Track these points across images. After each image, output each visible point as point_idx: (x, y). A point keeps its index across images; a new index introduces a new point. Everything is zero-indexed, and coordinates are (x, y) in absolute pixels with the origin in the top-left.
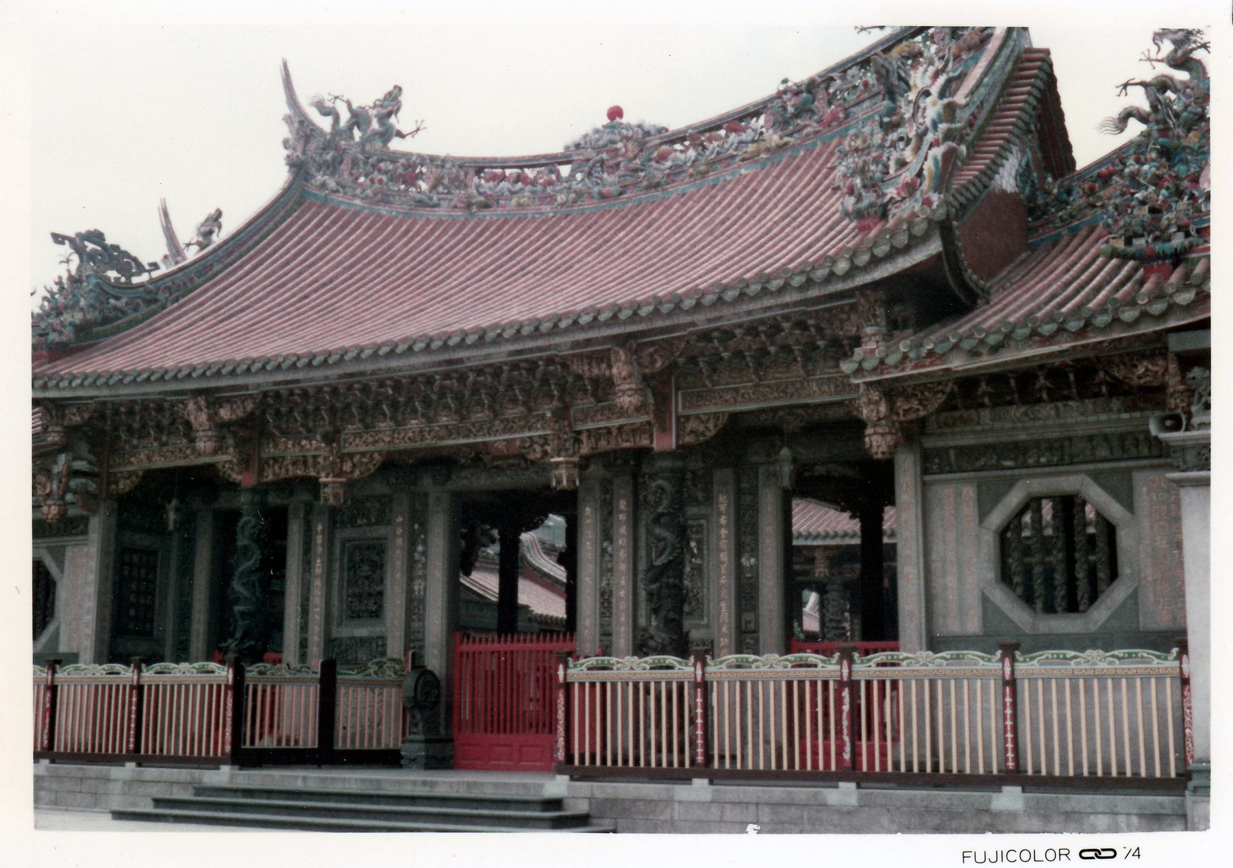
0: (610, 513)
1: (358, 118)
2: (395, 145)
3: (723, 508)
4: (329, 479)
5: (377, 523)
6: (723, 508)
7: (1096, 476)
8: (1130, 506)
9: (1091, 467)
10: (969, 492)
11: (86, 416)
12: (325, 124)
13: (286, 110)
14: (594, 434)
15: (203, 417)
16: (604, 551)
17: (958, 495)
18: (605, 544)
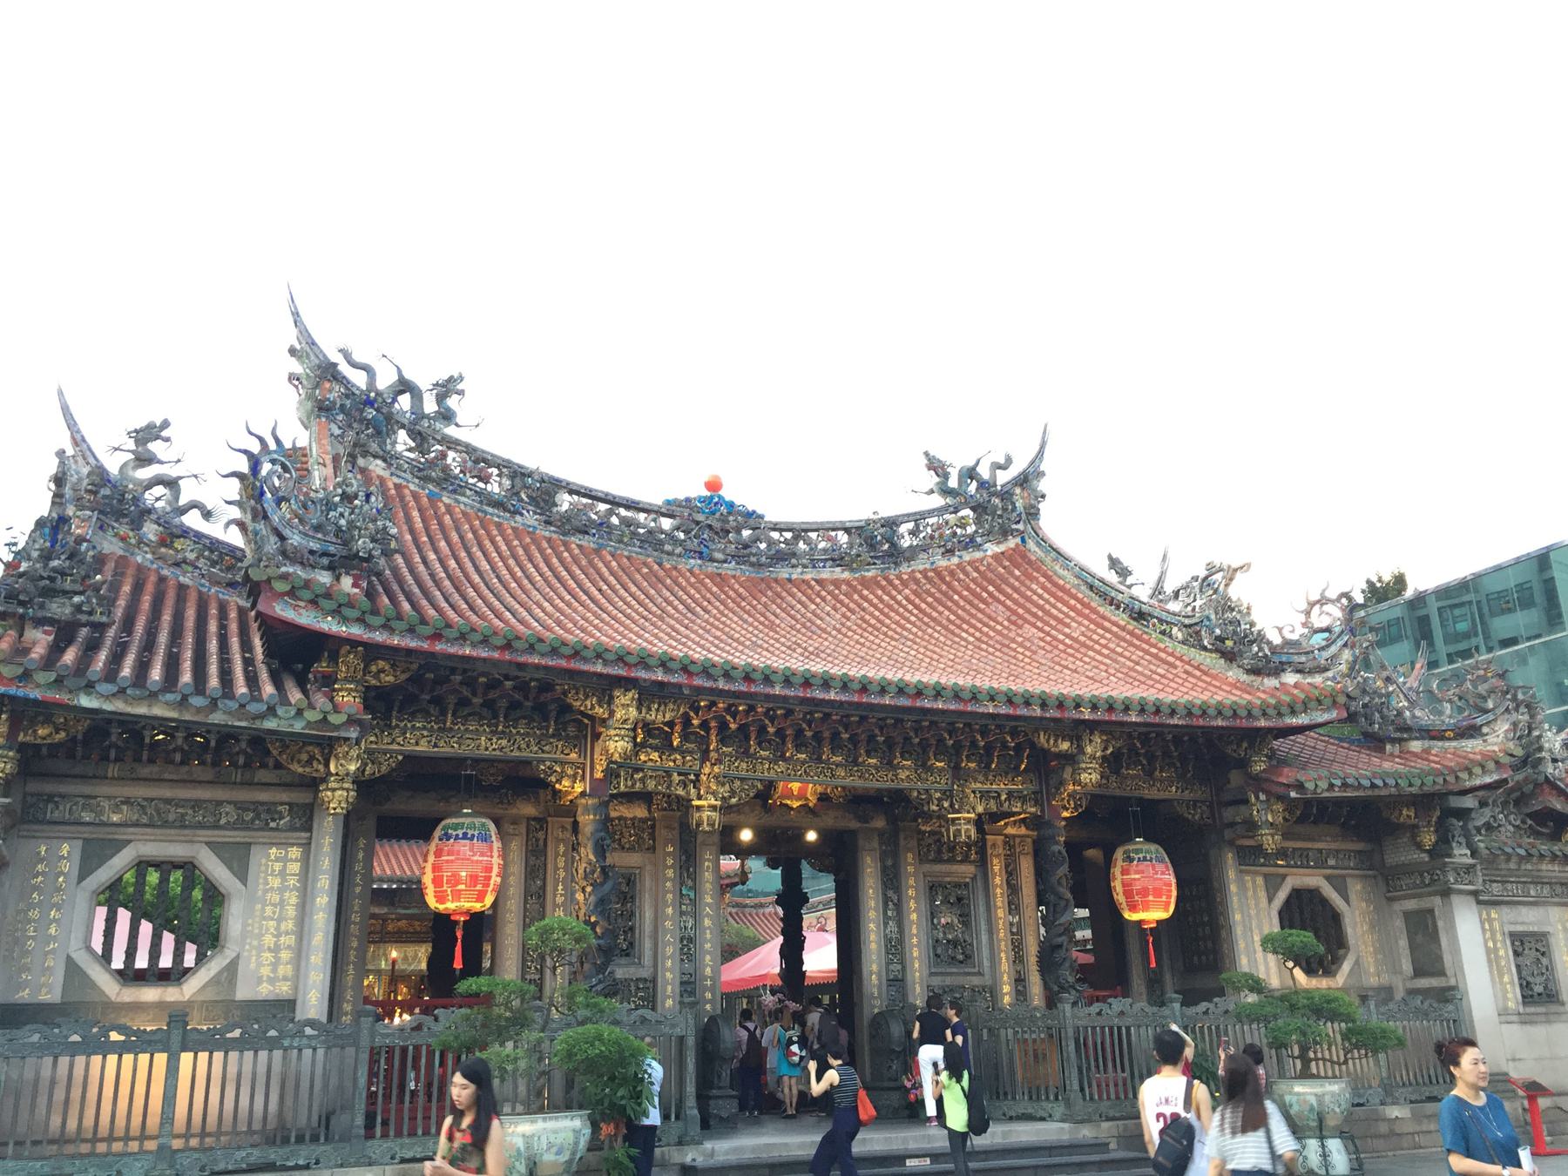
0: (896, 866)
1: (404, 386)
2: (451, 431)
3: (996, 868)
4: (713, 802)
5: (632, 849)
6: (996, 868)
7: (1328, 878)
8: (1347, 901)
9: (1329, 871)
10: (1260, 880)
11: (404, 677)
12: (359, 379)
13: (291, 337)
14: (985, 795)
15: (633, 712)
16: (886, 901)
17: (1254, 882)
18: (890, 893)
